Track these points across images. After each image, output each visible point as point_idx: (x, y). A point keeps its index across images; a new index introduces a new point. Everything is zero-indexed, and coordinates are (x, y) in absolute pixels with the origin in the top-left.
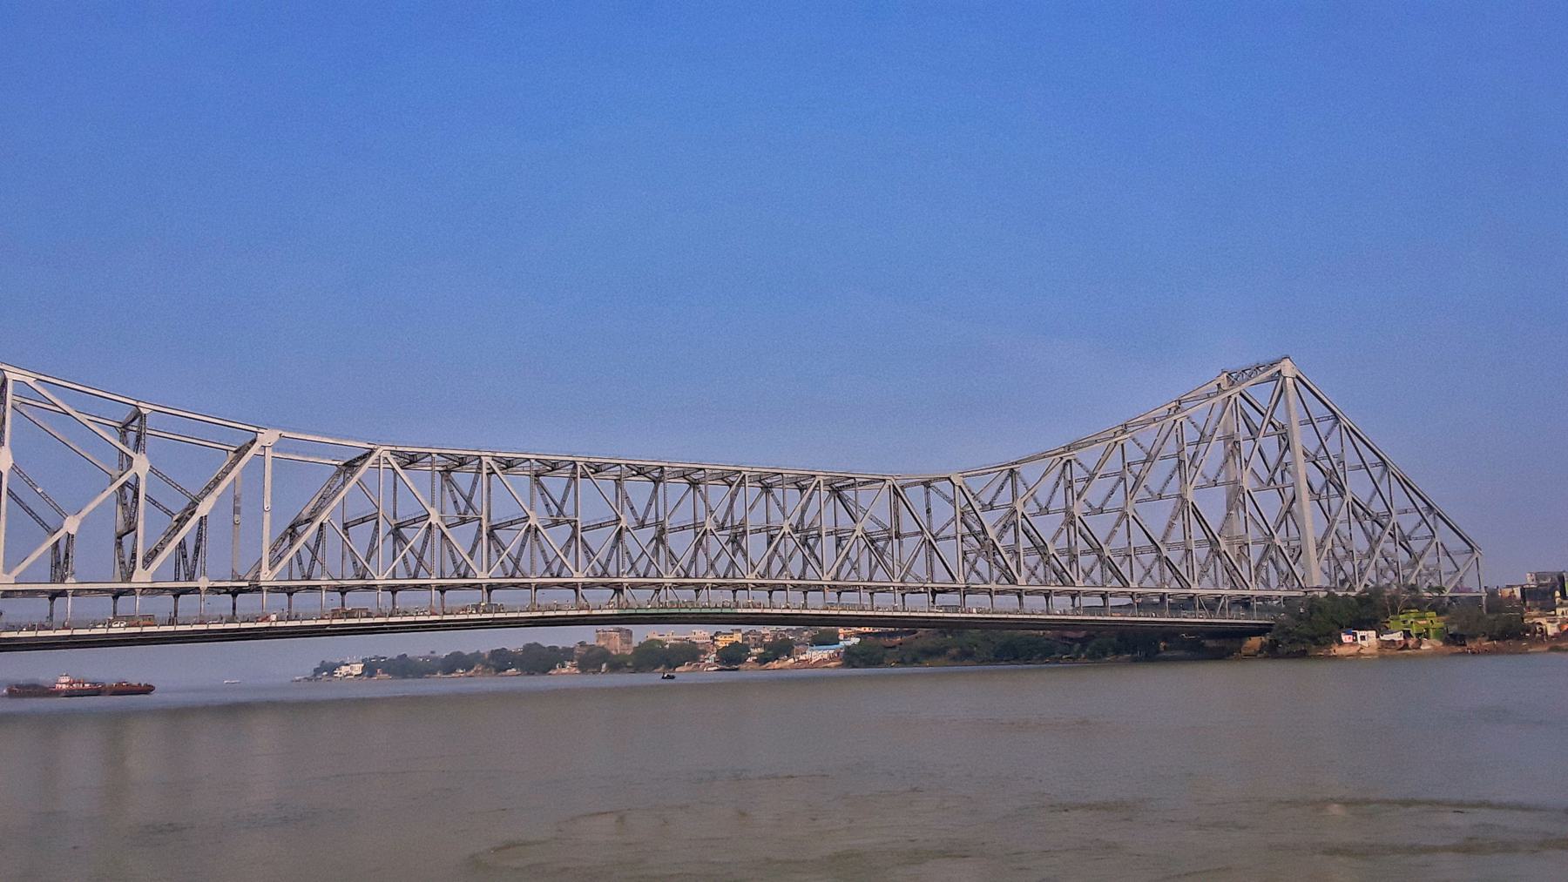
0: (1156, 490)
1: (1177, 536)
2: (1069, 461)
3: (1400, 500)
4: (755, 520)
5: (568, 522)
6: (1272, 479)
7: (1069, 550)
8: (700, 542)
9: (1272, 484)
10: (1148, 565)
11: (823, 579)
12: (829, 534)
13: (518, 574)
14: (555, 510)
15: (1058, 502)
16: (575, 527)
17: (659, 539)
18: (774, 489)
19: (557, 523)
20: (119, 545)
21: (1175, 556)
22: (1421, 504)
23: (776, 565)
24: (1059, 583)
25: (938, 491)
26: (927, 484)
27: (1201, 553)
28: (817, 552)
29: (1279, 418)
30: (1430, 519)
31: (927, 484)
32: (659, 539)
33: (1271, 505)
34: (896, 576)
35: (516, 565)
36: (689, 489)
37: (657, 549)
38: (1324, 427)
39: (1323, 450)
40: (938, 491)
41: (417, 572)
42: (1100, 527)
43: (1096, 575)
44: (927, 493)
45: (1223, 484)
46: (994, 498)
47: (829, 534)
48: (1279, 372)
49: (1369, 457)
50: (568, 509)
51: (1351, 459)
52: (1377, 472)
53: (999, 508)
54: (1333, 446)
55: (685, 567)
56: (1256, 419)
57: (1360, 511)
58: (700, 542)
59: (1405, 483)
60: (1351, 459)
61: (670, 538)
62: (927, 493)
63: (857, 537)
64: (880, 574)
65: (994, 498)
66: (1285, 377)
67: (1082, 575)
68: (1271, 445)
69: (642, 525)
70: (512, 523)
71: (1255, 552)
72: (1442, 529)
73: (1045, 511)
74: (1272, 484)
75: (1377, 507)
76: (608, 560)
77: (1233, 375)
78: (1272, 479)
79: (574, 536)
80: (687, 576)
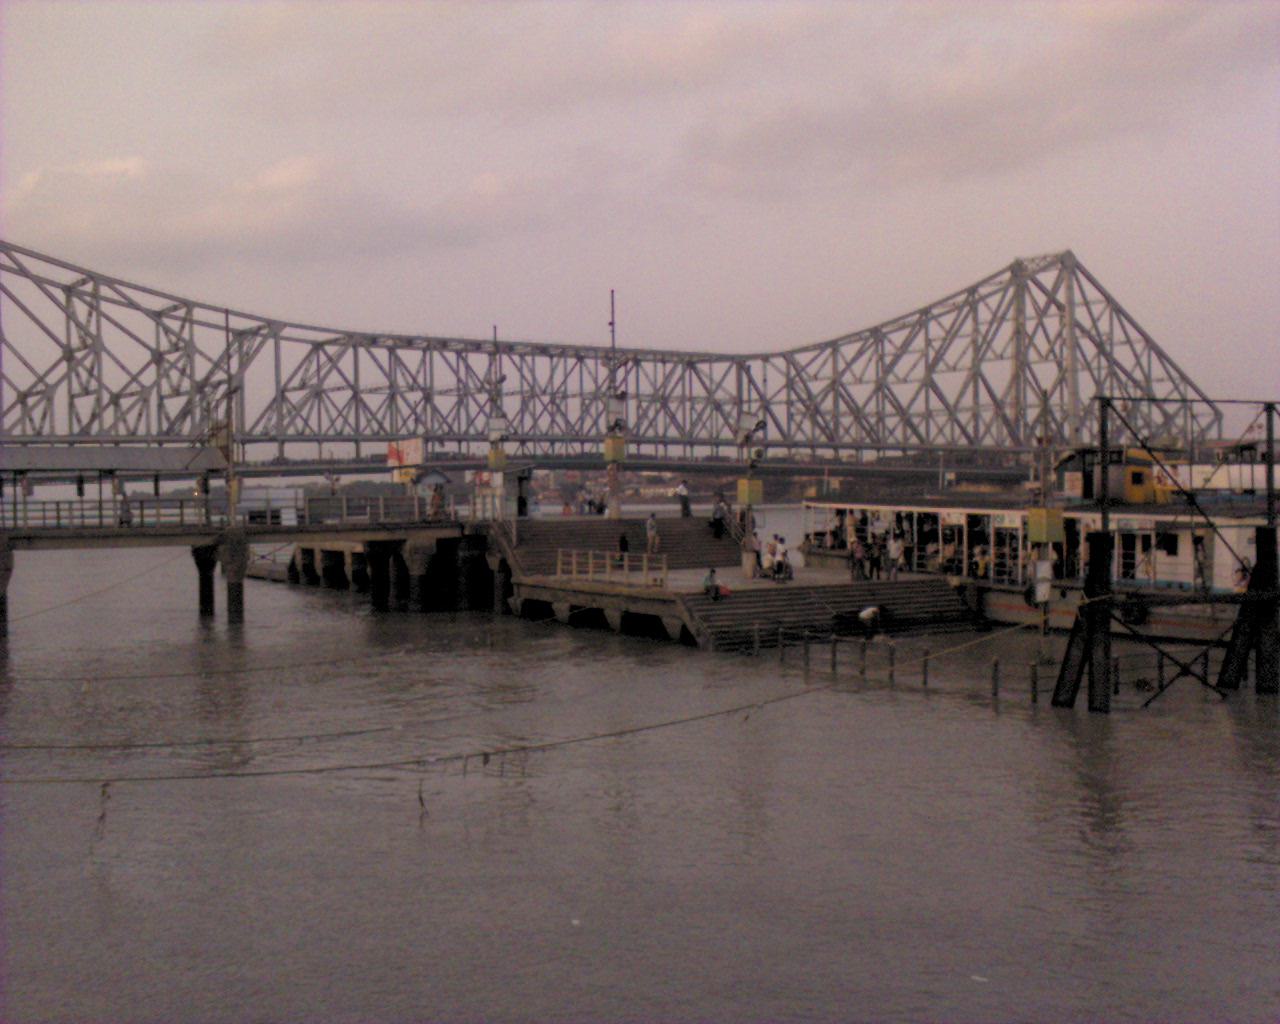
0: (951, 363)
3: (1157, 370)
4: (573, 386)
6: (1052, 351)
7: (877, 413)
21: (964, 417)
23: (588, 423)
25: (773, 365)
26: (765, 358)
27: (987, 415)
28: (563, 408)
30: (1182, 387)
33: (1046, 374)
40: (773, 365)
42: (904, 393)
44: (765, 368)
45: (1008, 358)
49: (1133, 334)
51: (1119, 335)
52: (1139, 347)
53: (822, 379)
54: (1103, 326)
60: (1119, 335)
62: (765, 368)
68: (1052, 324)
69: (544, 392)
73: (859, 381)
74: (1051, 357)
75: (1138, 375)
78: (1052, 351)
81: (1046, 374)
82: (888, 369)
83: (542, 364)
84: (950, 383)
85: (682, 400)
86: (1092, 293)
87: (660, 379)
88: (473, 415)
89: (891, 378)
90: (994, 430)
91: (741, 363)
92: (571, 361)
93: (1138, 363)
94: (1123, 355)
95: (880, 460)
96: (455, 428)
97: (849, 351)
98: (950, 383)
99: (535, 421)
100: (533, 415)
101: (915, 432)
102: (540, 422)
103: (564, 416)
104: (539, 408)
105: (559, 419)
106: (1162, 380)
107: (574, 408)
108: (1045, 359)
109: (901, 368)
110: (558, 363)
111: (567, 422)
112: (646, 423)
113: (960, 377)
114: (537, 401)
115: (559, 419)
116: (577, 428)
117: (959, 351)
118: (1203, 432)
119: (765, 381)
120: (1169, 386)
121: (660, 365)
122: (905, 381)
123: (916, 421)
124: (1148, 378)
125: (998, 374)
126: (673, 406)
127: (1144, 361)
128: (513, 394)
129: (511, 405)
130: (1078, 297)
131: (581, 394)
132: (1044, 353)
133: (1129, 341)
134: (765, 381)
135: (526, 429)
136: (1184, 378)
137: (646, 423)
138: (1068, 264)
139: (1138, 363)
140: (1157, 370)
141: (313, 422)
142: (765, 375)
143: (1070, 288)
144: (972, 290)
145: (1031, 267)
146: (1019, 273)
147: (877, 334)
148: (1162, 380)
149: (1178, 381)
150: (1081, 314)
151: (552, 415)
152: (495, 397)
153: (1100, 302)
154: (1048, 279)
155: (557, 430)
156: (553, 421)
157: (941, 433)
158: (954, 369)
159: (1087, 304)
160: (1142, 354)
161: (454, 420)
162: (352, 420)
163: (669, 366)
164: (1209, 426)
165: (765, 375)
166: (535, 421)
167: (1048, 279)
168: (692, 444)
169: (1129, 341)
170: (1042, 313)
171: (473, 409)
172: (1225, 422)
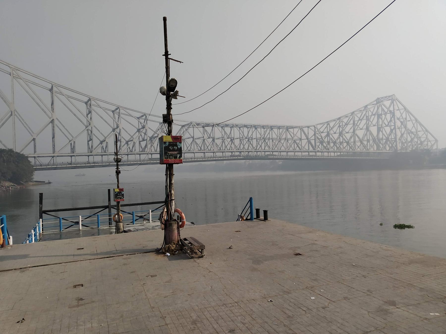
0: (361, 128)
2: (342, 121)
3: (419, 128)
4: (254, 136)
5: (212, 138)
8: (223, 141)
10: (359, 146)
11: (286, 150)
12: (271, 139)
13: (201, 150)
14: (209, 135)
15: (338, 131)
16: (193, 139)
17: (213, 140)
18: (273, 129)
19: (209, 138)
20: (88, 144)
21: (365, 143)
22: (424, 129)
24: (385, 150)
25: (311, 129)
26: (308, 127)
27: (371, 142)
28: (252, 143)
29: (391, 109)
32: (213, 140)
33: (388, 129)
34: (271, 148)
35: (201, 148)
36: (255, 130)
37: (213, 143)
39: (401, 117)
41: (225, 149)
43: (346, 148)
46: (324, 130)
47: (271, 139)
48: (392, 98)
50: (212, 135)
52: (414, 122)
54: (404, 116)
55: (238, 148)
56: (386, 110)
58: (223, 141)
59: (421, 124)
60: (408, 119)
61: (216, 141)
63: (278, 140)
64: (267, 148)
65: (324, 130)
67: (331, 148)
69: (246, 138)
70: (199, 138)
71: (384, 141)
73: (335, 133)
75: (414, 130)
76: (202, 146)
79: (193, 140)
80: (238, 150)
85: (269, 139)
86: (401, 107)
87: (263, 133)
91: (301, 128)
92: (254, 129)
94: (410, 125)
97: (332, 124)
98: (360, 133)
99: (244, 146)
103: (252, 145)
104: (245, 142)
105: (233, 146)
107: (237, 142)
108: (387, 126)
109: (347, 130)
110: (232, 128)
112: (259, 146)
115: (233, 146)
116: (238, 147)
118: (432, 146)
119: (308, 133)
121: (262, 129)
122: (348, 133)
124: (417, 131)
126: (267, 141)
127: (415, 125)
128: (237, 138)
129: (237, 142)
132: (387, 124)
134: (308, 133)
137: (259, 146)
140: (419, 128)
153: (403, 109)
156: (249, 146)
157: (359, 148)
158: (362, 129)
161: (221, 146)
163: (265, 129)
166: (226, 147)
170: (386, 114)
171: (226, 143)
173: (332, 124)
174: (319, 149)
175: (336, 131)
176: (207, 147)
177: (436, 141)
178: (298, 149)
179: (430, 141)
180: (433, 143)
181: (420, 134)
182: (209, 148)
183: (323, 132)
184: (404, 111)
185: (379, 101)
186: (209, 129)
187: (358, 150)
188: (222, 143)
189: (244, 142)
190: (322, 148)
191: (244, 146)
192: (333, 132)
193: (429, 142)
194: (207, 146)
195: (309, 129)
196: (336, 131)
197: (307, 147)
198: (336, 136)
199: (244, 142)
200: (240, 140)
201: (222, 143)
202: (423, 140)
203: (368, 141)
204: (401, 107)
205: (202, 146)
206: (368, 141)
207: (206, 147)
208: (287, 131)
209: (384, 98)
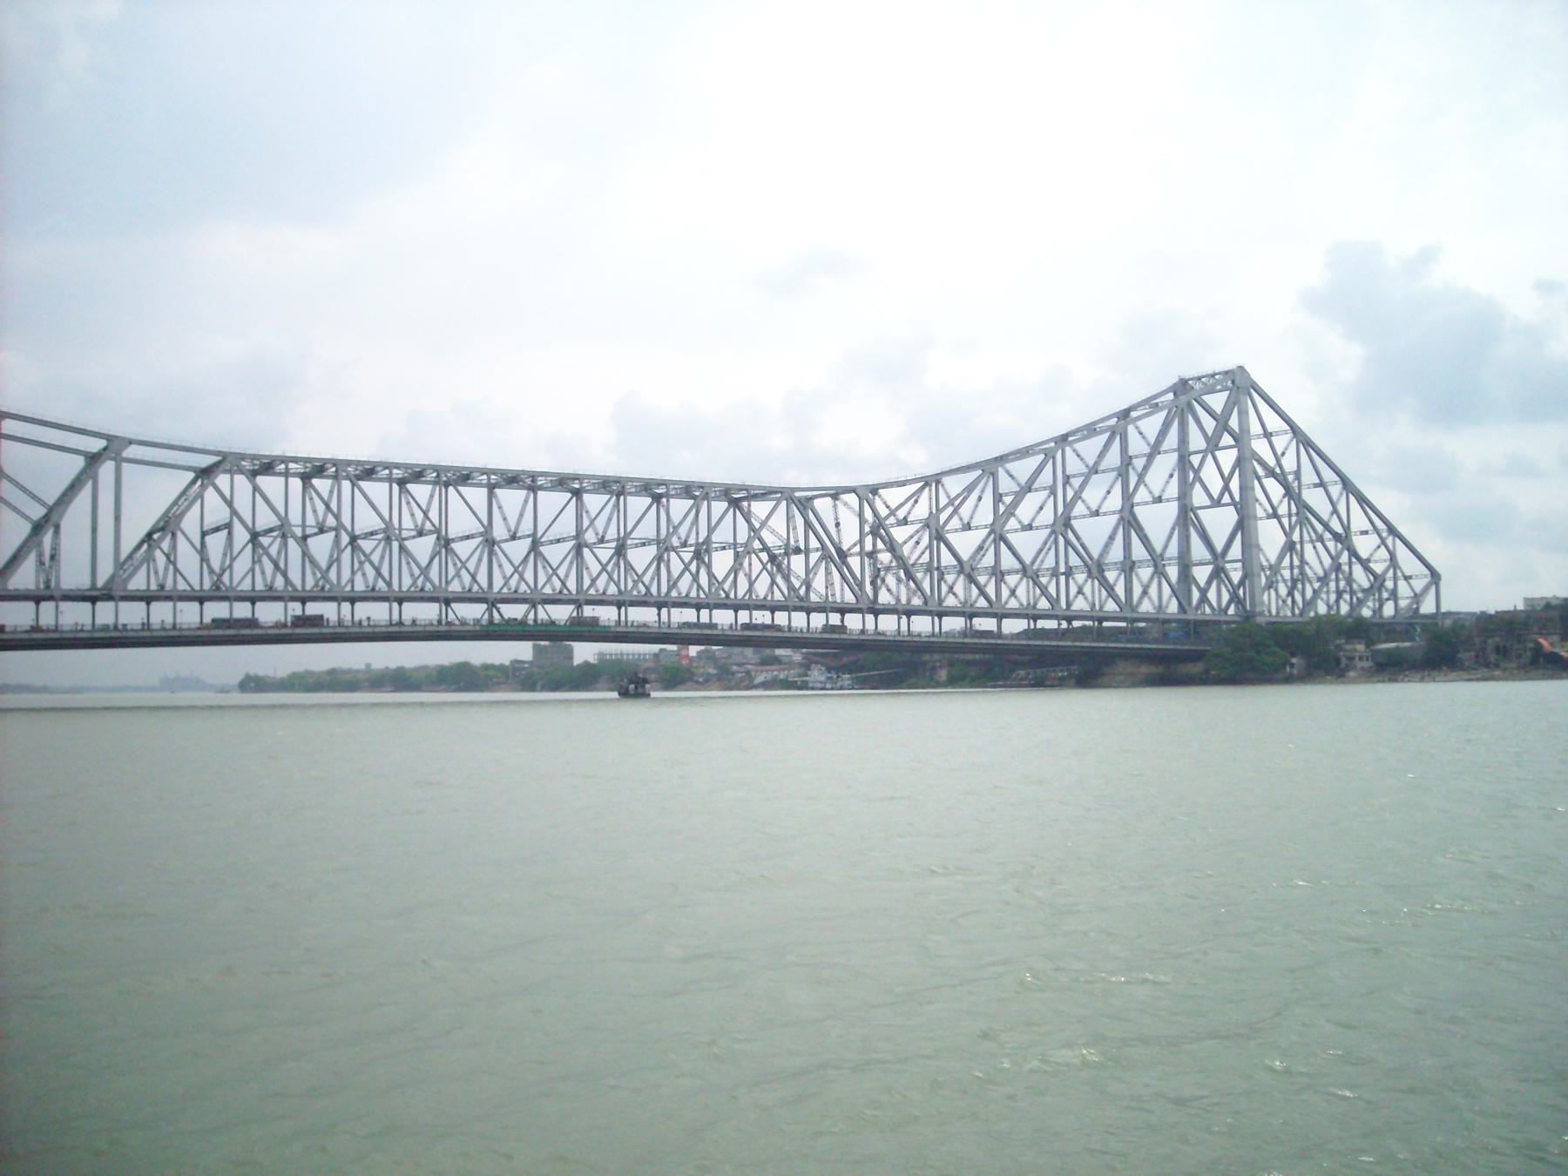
1: (1116, 553)
3: (1359, 520)
9: (1226, 499)
25: (846, 504)
26: (836, 494)
30: (1389, 541)
31: (835, 497)
33: (1220, 522)
38: (1280, 442)
40: (846, 504)
44: (835, 506)
49: (1328, 475)
52: (1336, 490)
53: (913, 523)
57: (1319, 528)
59: (1363, 500)
60: (1308, 476)
62: (835, 506)
66: (1238, 388)
72: (1402, 552)
77: (1190, 382)
81: (1220, 522)
82: (1011, 512)
83: (511, 499)
84: (1094, 532)
86: (1274, 423)
88: (675, 574)
89: (1012, 523)
90: (1153, 590)
91: (800, 502)
92: (719, 507)
93: (1335, 511)
95: (1026, 633)
96: (654, 590)
97: (954, 485)
98: (1094, 532)
99: (751, 584)
100: (748, 576)
101: (1044, 591)
102: (756, 585)
103: (787, 578)
104: (757, 566)
106: (1365, 533)
108: (1217, 503)
109: (1025, 510)
111: (791, 587)
113: (1108, 522)
114: (753, 555)
117: (1102, 494)
118: (1417, 598)
119: (838, 525)
120: (1373, 540)
123: (1044, 580)
124: (1347, 528)
125: (1158, 520)
129: (640, 558)
130: (1255, 428)
131: (735, 545)
132: (1215, 494)
133: (1322, 484)
134: (838, 525)
135: (741, 593)
136: (1392, 530)
138: (1239, 384)
139: (1335, 511)
140: (1359, 520)
141: (482, 578)
142: (836, 519)
143: (1243, 414)
144: (1124, 415)
145: (1198, 386)
146: (1184, 395)
147: (990, 468)
148: (1365, 533)
149: (1384, 534)
150: (1260, 447)
151: (771, 574)
152: (702, 553)
153: (1286, 432)
154: (1217, 401)
155: (778, 596)
156: (773, 582)
157: (1274, 604)
159: (1267, 435)
160: (1339, 499)
161: (652, 579)
162: (529, 576)
164: (1426, 589)
165: (836, 519)
167: (1217, 401)
168: (876, 611)
169: (1322, 484)
170: (1213, 445)
171: (676, 567)
172: (1442, 584)
173: (954, 485)
174: (1013, 604)
175: (972, 518)
176: (594, 581)
177: (1435, 576)
178: (982, 603)
179: (1407, 578)
180: (1418, 585)
181: (1364, 545)
182: (601, 583)
183: (905, 518)
184: (1291, 441)
185: (1182, 387)
186: (420, 491)
187: (1008, 606)
188: (658, 568)
189: (750, 565)
190: (1093, 597)
191: (751, 584)
192: (960, 522)
193: (1402, 584)
194: (590, 574)
195: (837, 502)
196: (972, 518)
197: (762, 588)
198: (1027, 544)
199: (750, 565)
200: (737, 555)
201: (658, 568)
202: (1378, 568)
203: (1128, 567)
204: (1274, 423)
205: (567, 576)
206: (1128, 567)
207: (587, 582)
208: (737, 511)
209: (1203, 380)
